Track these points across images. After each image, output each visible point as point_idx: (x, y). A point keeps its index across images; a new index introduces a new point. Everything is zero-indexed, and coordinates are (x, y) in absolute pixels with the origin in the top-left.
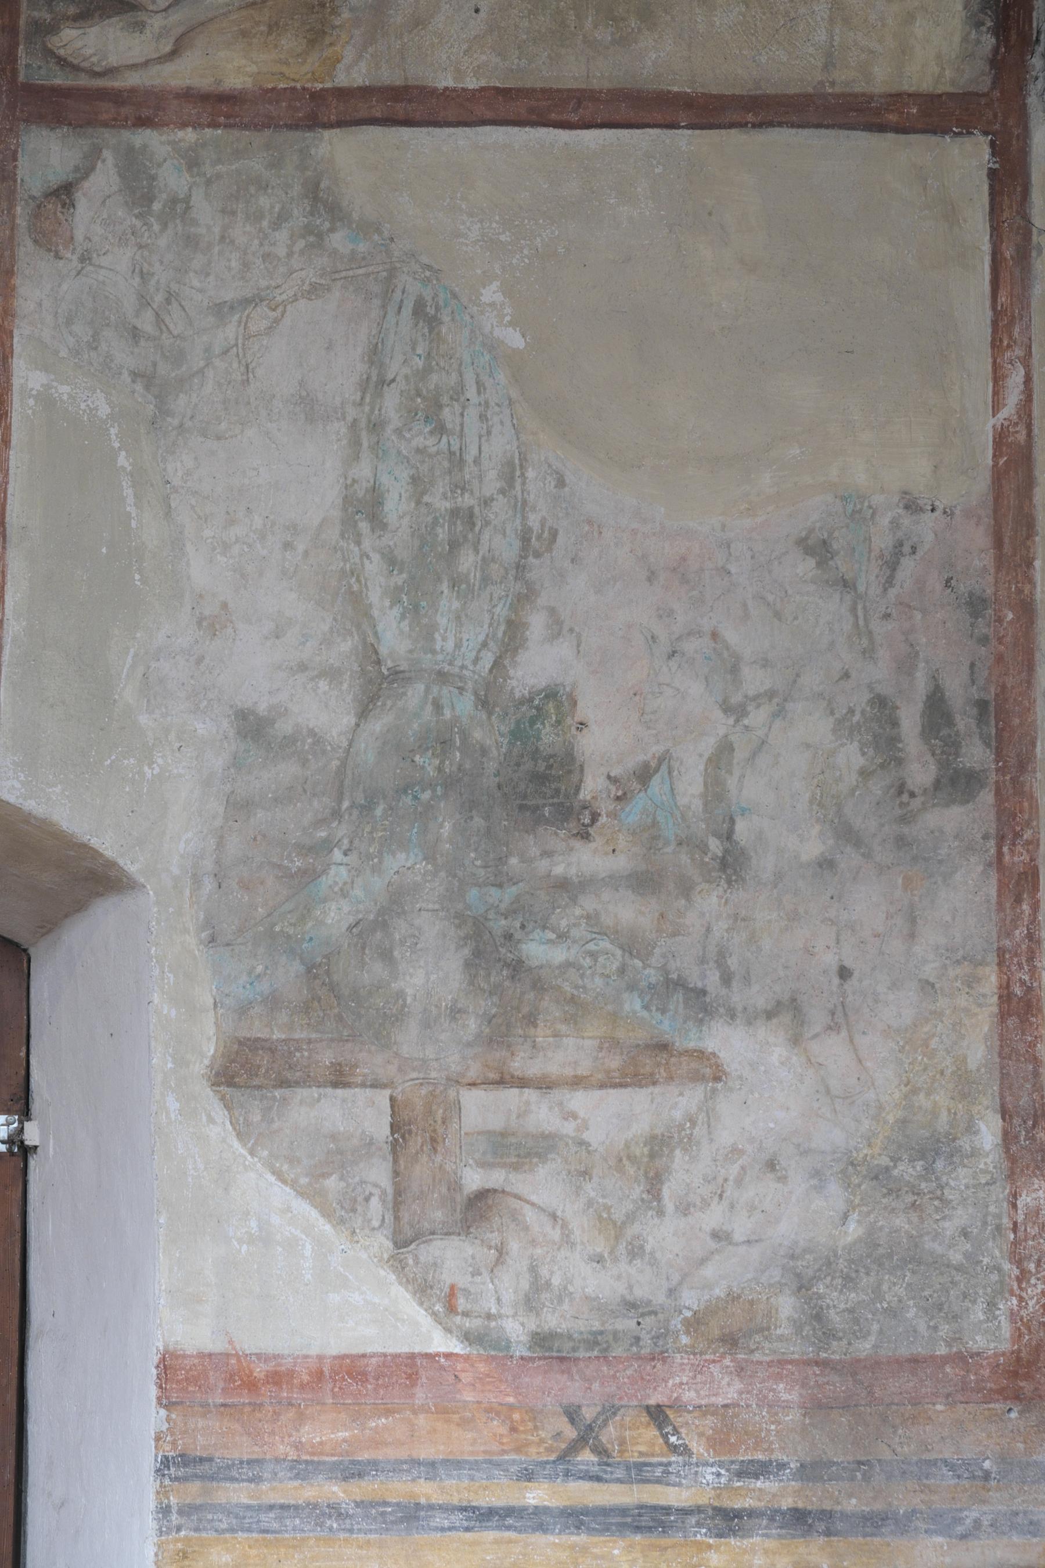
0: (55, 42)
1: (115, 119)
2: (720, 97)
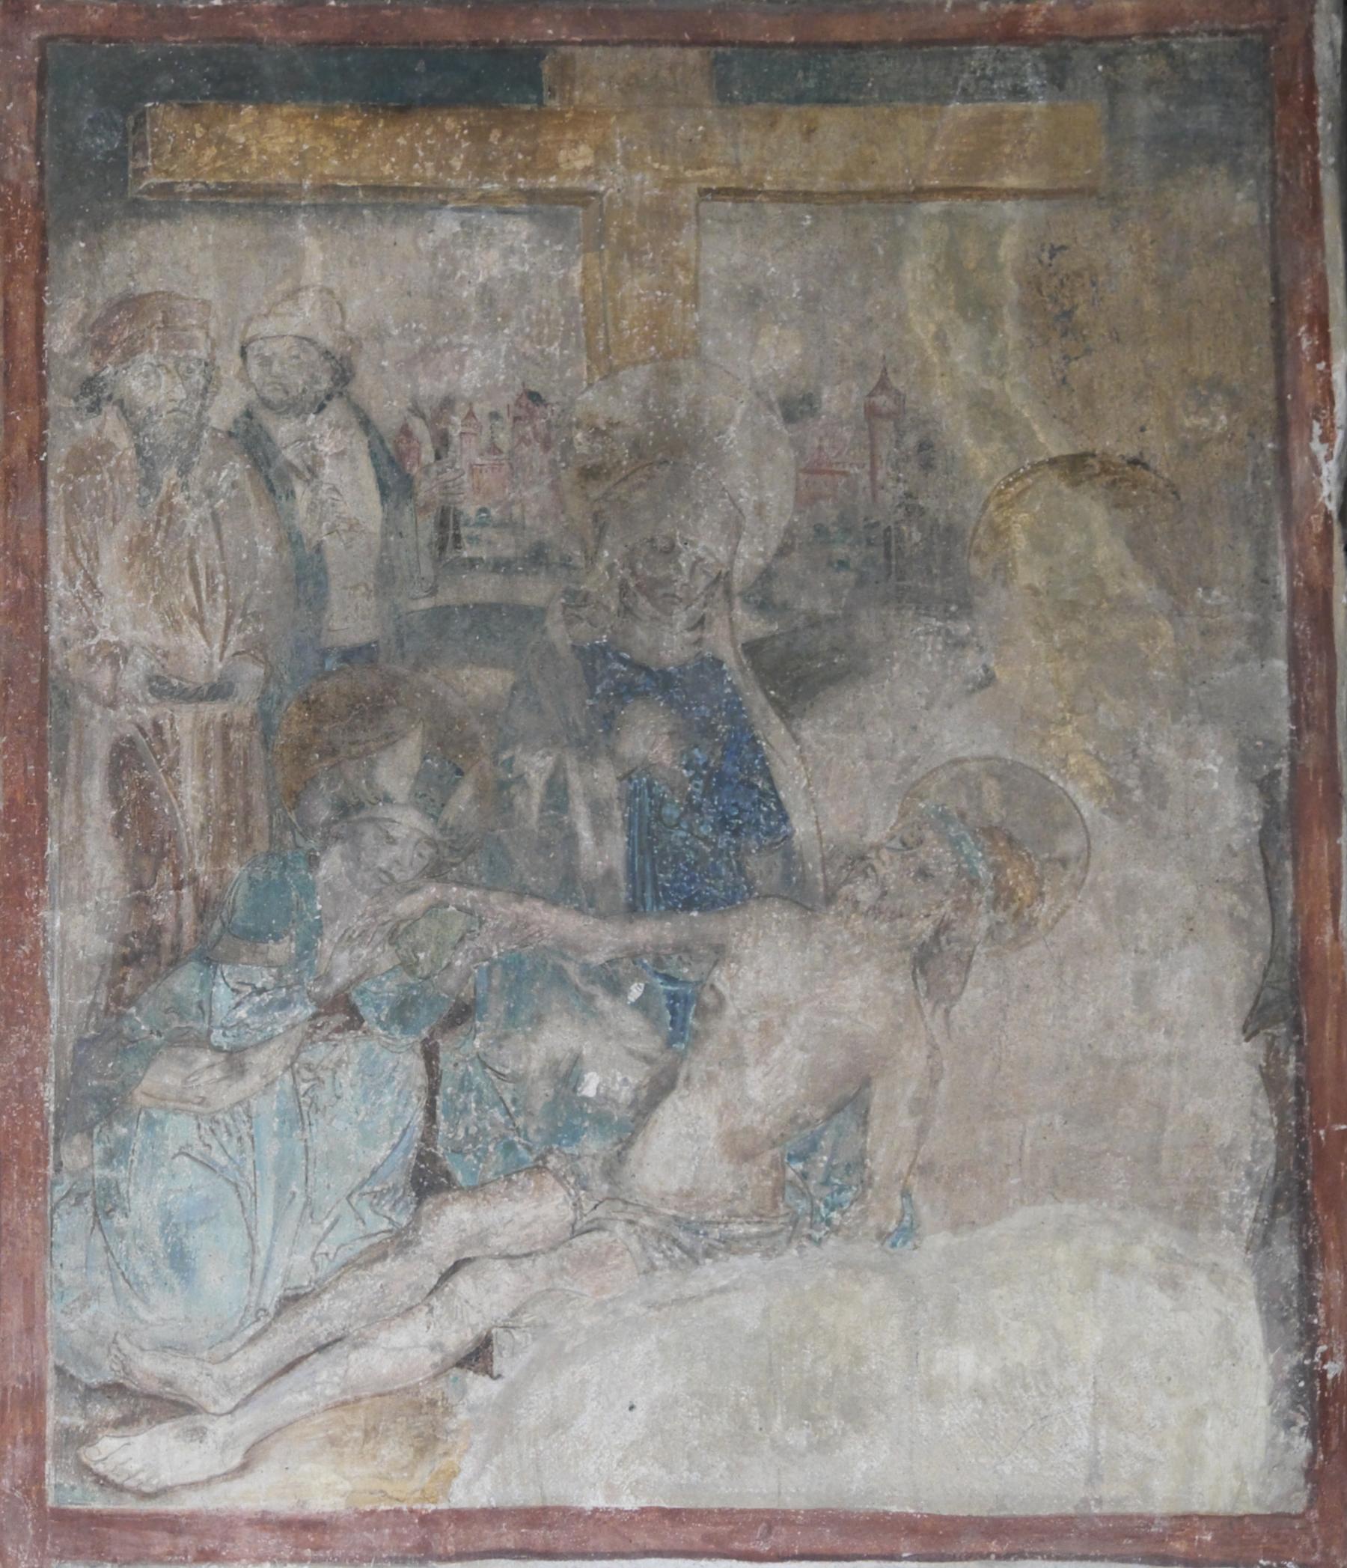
0: (91, 1455)
1: (171, 1553)
2: (952, 1519)
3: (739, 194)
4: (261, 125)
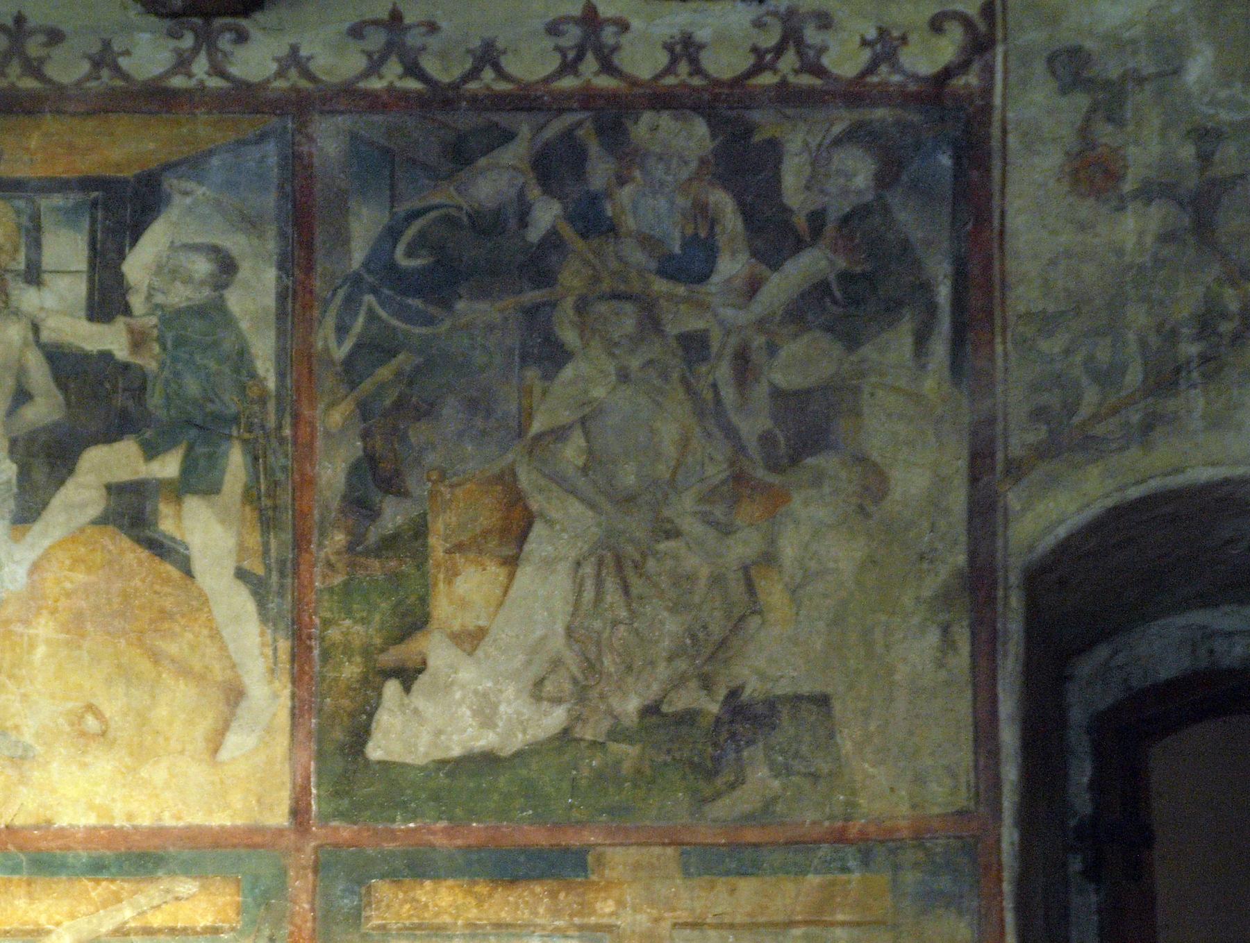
3: (694, 925)
4: (435, 891)
